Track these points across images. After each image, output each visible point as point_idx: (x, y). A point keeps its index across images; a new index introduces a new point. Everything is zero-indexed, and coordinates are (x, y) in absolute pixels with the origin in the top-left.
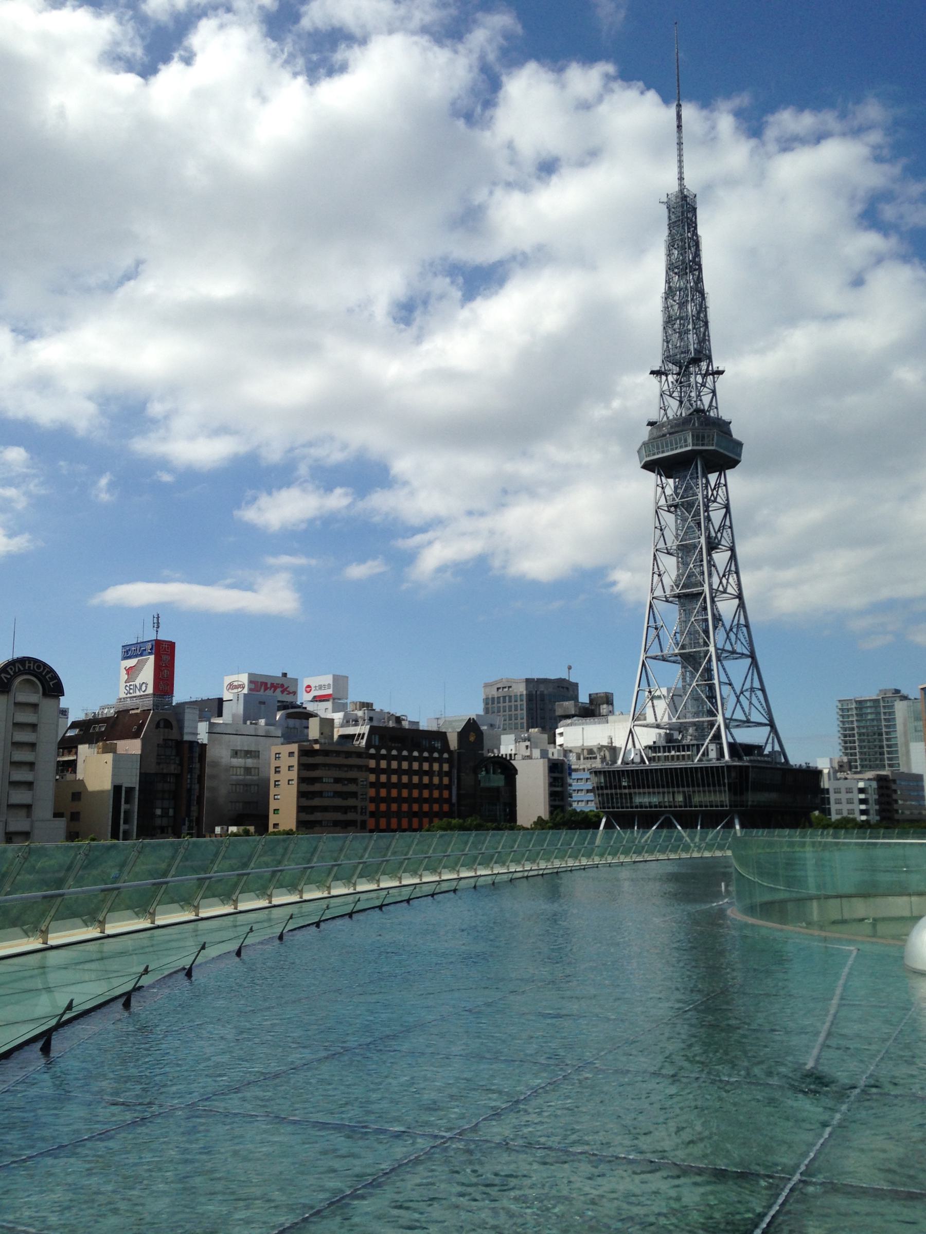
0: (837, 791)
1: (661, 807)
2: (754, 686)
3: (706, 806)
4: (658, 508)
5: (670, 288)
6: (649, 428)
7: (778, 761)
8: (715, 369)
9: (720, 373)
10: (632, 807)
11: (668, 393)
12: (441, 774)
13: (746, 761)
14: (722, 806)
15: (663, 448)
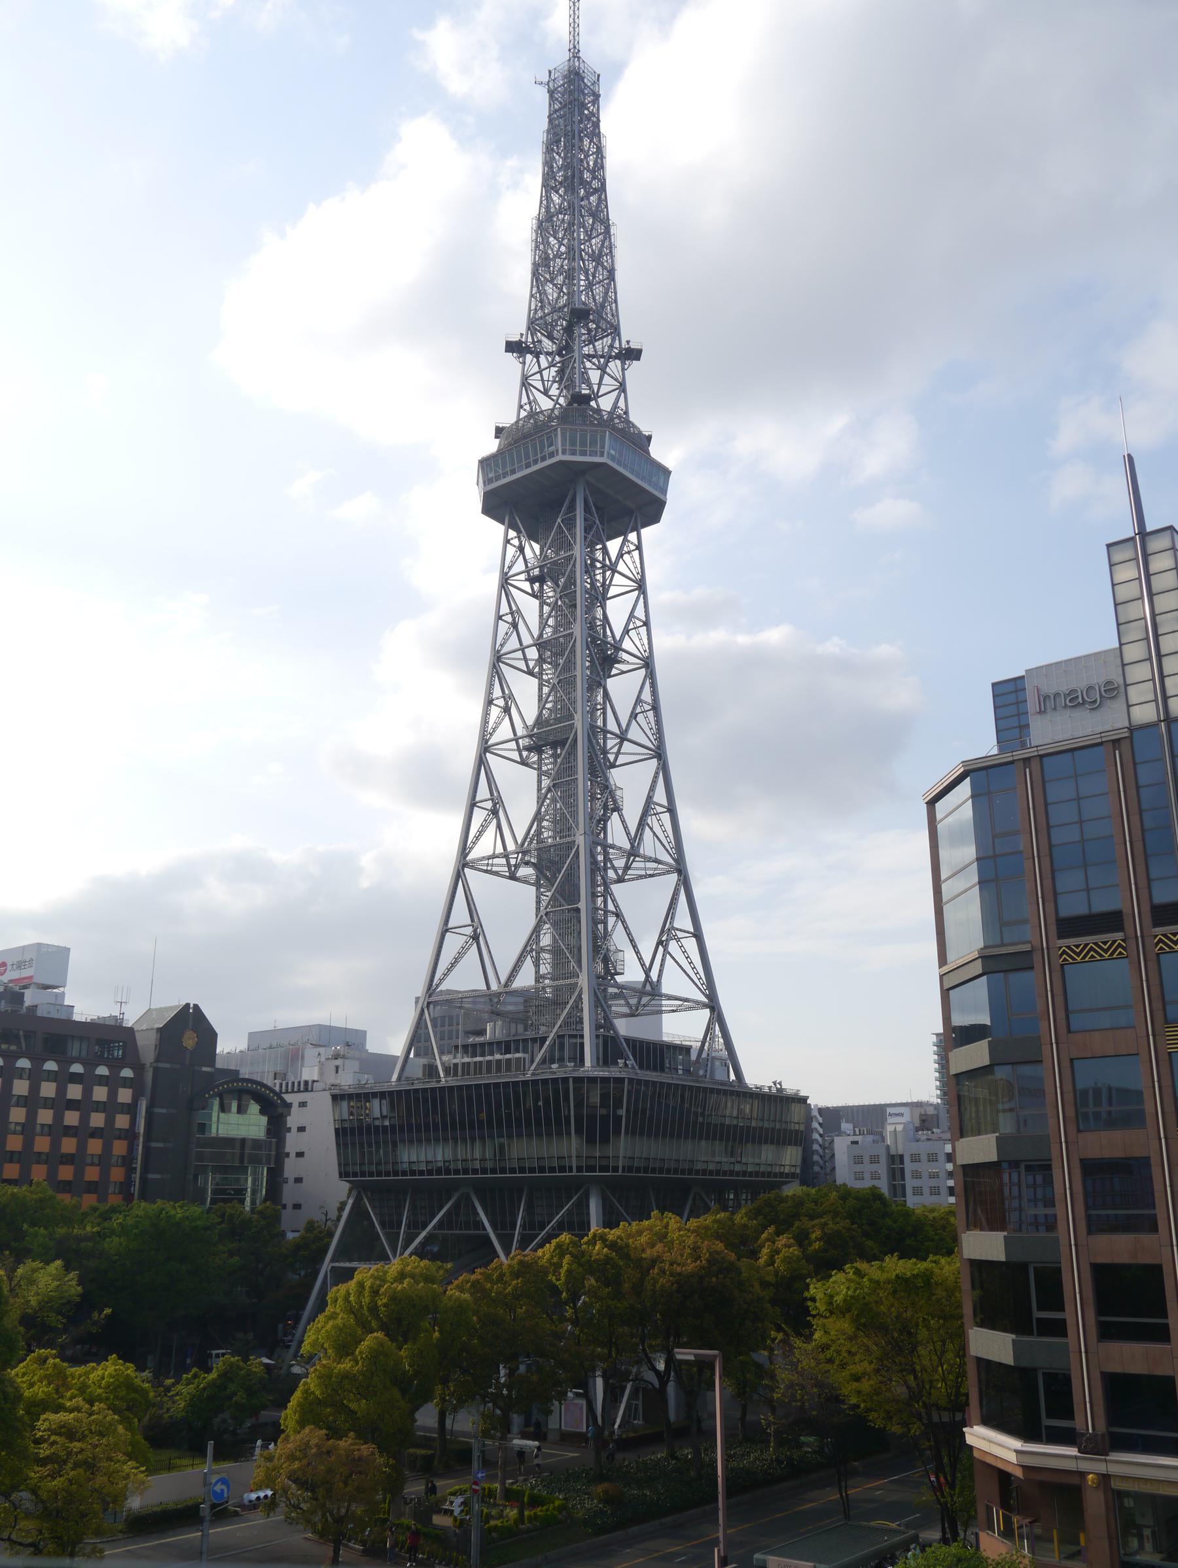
0: (916, 1158)
1: (448, 1172)
2: (676, 925)
3: (532, 1170)
4: (505, 581)
5: (548, 208)
6: (498, 441)
7: (719, 1076)
8: (624, 345)
9: (632, 354)
10: (396, 1173)
11: (539, 385)
12: (110, 1107)
13: (625, 1069)
14: (562, 1169)
15: (513, 464)
